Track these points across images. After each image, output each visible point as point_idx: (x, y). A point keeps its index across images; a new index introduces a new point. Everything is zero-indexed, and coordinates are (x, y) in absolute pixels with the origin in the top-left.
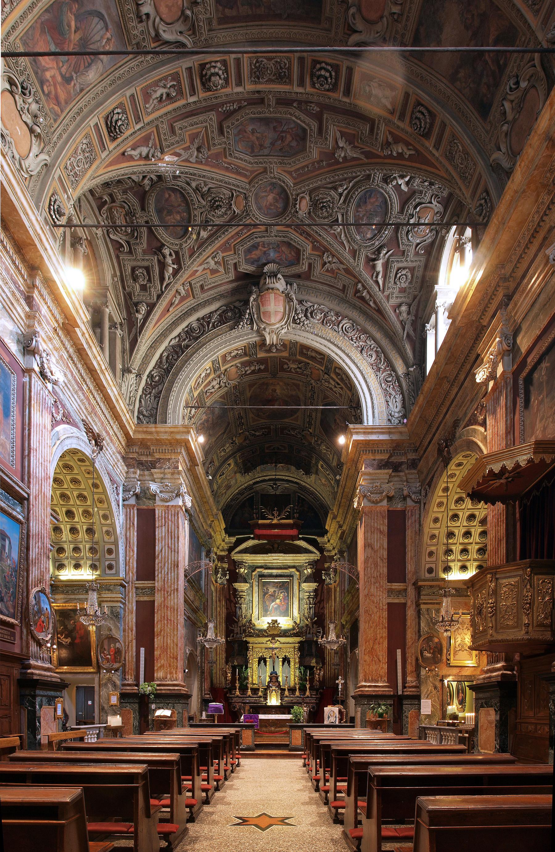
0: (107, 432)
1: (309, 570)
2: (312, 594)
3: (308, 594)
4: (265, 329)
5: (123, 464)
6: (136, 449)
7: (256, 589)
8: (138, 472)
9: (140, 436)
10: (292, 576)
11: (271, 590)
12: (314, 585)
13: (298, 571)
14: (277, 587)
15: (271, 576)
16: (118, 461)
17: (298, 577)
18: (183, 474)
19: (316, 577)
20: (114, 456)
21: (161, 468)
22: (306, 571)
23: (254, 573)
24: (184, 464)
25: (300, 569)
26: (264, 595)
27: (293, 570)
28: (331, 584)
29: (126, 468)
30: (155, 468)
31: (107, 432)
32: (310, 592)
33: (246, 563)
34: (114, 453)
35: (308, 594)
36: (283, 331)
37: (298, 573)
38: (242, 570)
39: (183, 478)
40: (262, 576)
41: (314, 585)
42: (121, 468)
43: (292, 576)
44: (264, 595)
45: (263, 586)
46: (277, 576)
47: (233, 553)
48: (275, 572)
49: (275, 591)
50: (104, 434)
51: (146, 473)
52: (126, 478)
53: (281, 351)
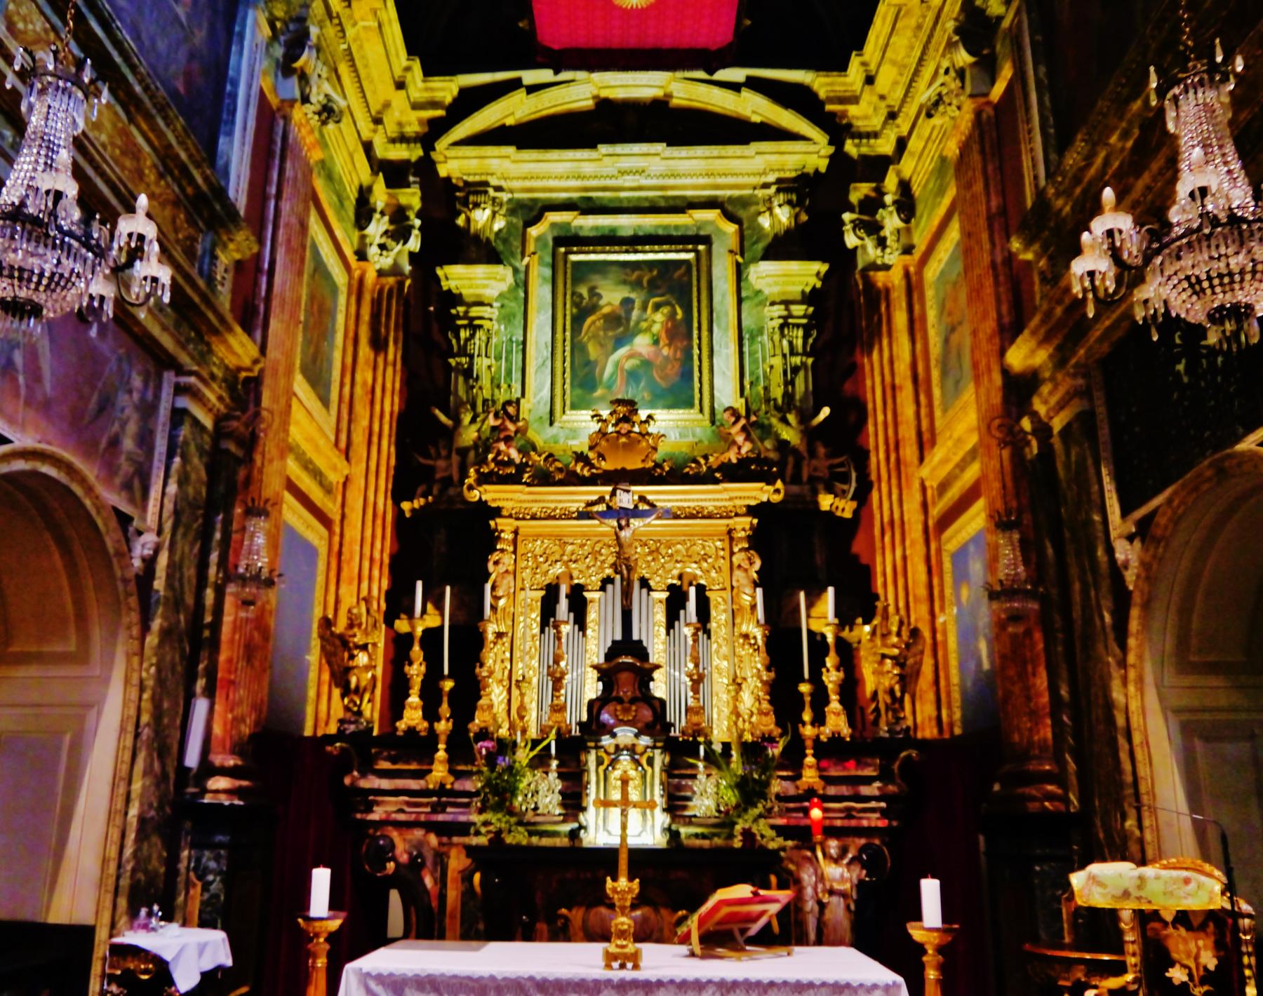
1: (784, 216)
2: (798, 310)
3: (779, 310)
7: (540, 293)
10: (707, 240)
11: (612, 295)
12: (804, 274)
13: (731, 217)
14: (636, 285)
15: (609, 240)
17: (733, 243)
19: (812, 236)
22: (765, 222)
23: (534, 232)
25: (742, 214)
26: (578, 321)
27: (712, 215)
28: (887, 267)
32: (787, 303)
33: (499, 189)
35: (779, 310)
37: (731, 228)
38: (480, 217)
40: (568, 239)
41: (804, 274)
43: (707, 240)
44: (578, 321)
45: (576, 281)
46: (636, 241)
47: (442, 145)
48: (626, 224)
49: (627, 303)
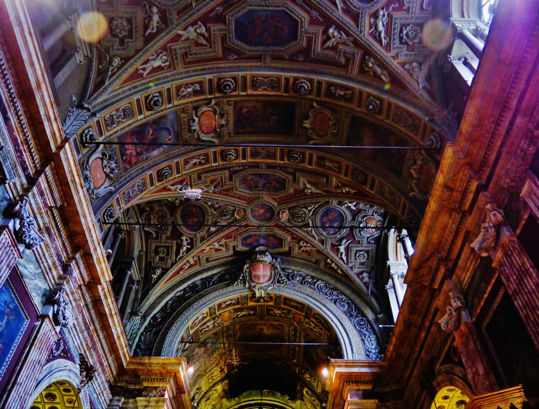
0: (102, 364)
4: (255, 286)
5: (109, 392)
6: (126, 378)
8: (123, 399)
9: (132, 367)
16: (105, 389)
18: (168, 402)
20: (101, 386)
21: (146, 396)
24: (170, 392)
29: (111, 396)
30: (141, 396)
31: (102, 364)
34: (102, 383)
36: (270, 288)
39: (167, 405)
42: (106, 396)
50: (98, 365)
51: (131, 401)
52: (108, 406)
53: (268, 301)
